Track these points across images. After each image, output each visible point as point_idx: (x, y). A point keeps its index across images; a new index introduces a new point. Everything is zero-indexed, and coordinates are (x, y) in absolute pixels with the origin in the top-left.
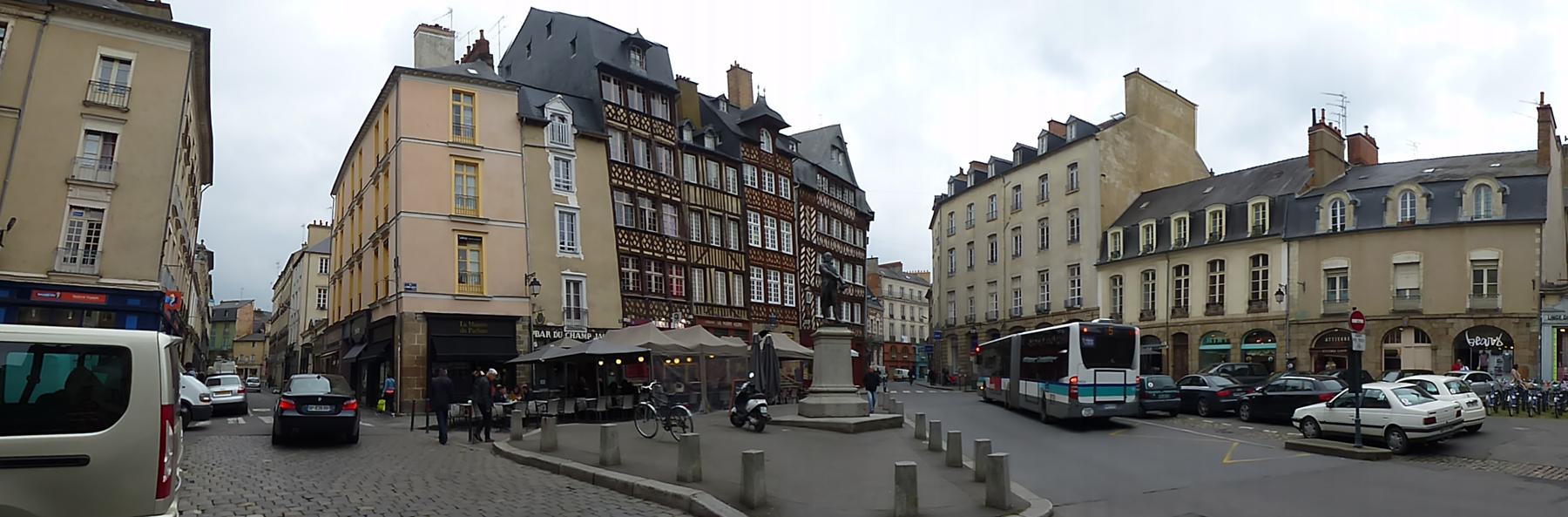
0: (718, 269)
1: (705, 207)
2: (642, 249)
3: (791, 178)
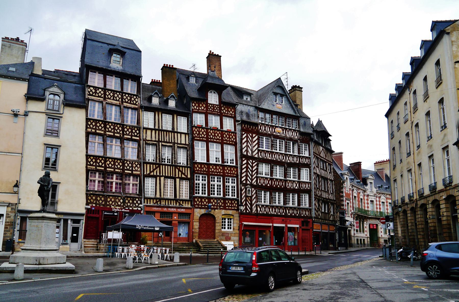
0: (166, 177)
2: (105, 167)
3: (234, 118)
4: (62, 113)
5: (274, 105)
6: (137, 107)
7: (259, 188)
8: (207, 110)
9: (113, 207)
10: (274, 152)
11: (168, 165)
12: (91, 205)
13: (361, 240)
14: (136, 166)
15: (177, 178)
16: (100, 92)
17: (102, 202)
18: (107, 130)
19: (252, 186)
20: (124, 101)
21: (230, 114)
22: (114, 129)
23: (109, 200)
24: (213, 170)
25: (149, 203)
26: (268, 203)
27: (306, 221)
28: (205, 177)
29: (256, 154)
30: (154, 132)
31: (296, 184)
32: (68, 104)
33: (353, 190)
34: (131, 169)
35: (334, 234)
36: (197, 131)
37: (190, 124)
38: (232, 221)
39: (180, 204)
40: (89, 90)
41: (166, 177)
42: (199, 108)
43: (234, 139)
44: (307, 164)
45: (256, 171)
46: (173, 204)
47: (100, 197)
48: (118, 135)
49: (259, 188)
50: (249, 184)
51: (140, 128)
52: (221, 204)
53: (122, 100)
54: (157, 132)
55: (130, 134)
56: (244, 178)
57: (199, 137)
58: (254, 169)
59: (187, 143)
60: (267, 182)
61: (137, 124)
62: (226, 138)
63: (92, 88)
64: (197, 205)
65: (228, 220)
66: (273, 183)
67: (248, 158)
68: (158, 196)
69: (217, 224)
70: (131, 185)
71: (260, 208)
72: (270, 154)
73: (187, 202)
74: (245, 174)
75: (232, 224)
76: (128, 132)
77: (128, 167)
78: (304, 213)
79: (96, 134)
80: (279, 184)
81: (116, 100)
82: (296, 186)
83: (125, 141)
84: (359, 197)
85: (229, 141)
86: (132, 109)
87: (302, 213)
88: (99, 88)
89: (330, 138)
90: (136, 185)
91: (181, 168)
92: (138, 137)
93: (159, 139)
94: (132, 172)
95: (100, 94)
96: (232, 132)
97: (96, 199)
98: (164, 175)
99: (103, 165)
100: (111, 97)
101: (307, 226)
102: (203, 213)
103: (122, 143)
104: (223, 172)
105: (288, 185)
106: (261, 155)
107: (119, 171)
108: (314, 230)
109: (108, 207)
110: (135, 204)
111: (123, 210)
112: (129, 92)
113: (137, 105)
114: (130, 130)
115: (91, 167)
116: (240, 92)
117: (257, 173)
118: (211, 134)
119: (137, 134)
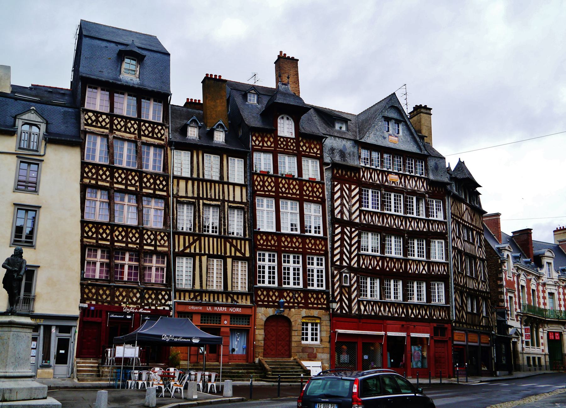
0: (210, 256)
2: (112, 241)
3: (321, 159)
4: (42, 153)
5: (385, 138)
6: (162, 142)
7: (363, 273)
8: (276, 147)
9: (124, 305)
10: (386, 214)
11: (213, 237)
12: (88, 302)
13: (534, 358)
14: (162, 238)
15: (229, 257)
16: (104, 120)
17: (107, 297)
18: (115, 180)
19: (350, 269)
20: (142, 133)
21: (314, 153)
23: (118, 294)
24: (286, 243)
25: (182, 298)
26: (377, 298)
27: (441, 328)
28: (274, 256)
29: (356, 218)
30: (190, 183)
31: (424, 267)
32: (53, 139)
33: (519, 276)
34: (153, 243)
35: (489, 348)
36: (261, 180)
37: (248, 170)
38: (318, 327)
39: (233, 300)
40: (87, 117)
41: (210, 256)
42: (263, 144)
43: (320, 194)
44: (441, 232)
45: (356, 245)
46: (222, 300)
47: (103, 290)
48: (133, 189)
49: (363, 273)
50: (345, 267)
51: (168, 177)
52: (299, 299)
53: (139, 132)
54: (196, 183)
55: (152, 187)
56: (338, 257)
57: (264, 191)
58: (353, 243)
60: (376, 263)
61: (164, 170)
62: (308, 192)
63: (90, 114)
64: (261, 301)
65: (312, 325)
66: (386, 264)
67: (343, 223)
68: (197, 287)
69: (293, 333)
70: (154, 269)
71: (365, 307)
72: (379, 218)
73: (244, 297)
74: (338, 250)
75: (318, 332)
76: (148, 184)
77: (149, 241)
78: (437, 314)
79: (96, 187)
80: (395, 267)
81: (130, 133)
82: (424, 269)
83: (144, 198)
84: (529, 288)
85: (313, 196)
86: (155, 146)
87: (434, 314)
88: (102, 114)
89: (478, 189)
90: (162, 269)
91: (234, 241)
92: (164, 191)
93: (198, 194)
95: (104, 124)
96: (318, 183)
97: (97, 293)
98: (207, 252)
99: (109, 238)
100: (122, 127)
101: (443, 334)
102: (271, 314)
103: (139, 201)
104: (304, 247)
105: (410, 268)
106: (365, 218)
107: (135, 246)
108: (455, 342)
109: (117, 305)
110: (160, 300)
111: (141, 310)
112: (151, 119)
113: (163, 140)
114: (152, 181)
115: (88, 240)
116: (329, 117)
117: (359, 248)
118: (284, 186)
119: (164, 186)
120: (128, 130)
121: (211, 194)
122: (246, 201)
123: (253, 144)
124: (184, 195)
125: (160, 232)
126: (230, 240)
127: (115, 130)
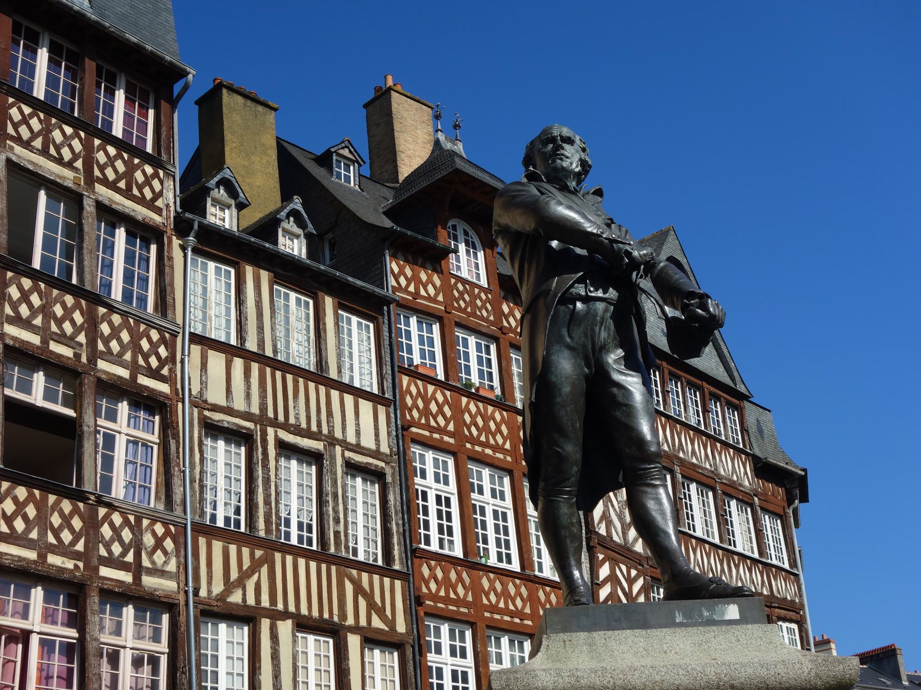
1: (262, 420)
15: (356, 629)
20: (97, 173)
22: (45, 310)
34: (130, 558)
42: (417, 289)
57: (427, 427)
59: (384, 449)
76: (114, 346)
77: (117, 549)
81: (59, 161)
92: (163, 379)
93: (263, 407)
94: (137, 578)
100: (34, 136)
107: (69, 564)
113: (158, 211)
119: (162, 362)
120: (52, 151)
121: (298, 414)
122: (387, 451)
123: (394, 283)
124: (222, 402)
125: (154, 521)
126: (354, 572)
127: (12, 138)
